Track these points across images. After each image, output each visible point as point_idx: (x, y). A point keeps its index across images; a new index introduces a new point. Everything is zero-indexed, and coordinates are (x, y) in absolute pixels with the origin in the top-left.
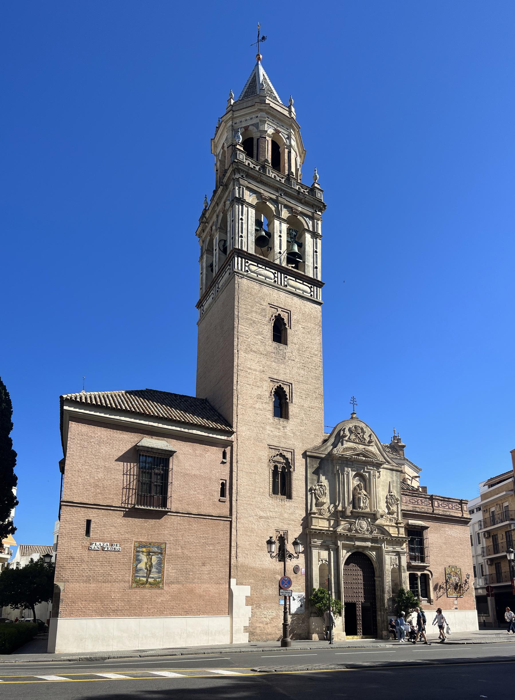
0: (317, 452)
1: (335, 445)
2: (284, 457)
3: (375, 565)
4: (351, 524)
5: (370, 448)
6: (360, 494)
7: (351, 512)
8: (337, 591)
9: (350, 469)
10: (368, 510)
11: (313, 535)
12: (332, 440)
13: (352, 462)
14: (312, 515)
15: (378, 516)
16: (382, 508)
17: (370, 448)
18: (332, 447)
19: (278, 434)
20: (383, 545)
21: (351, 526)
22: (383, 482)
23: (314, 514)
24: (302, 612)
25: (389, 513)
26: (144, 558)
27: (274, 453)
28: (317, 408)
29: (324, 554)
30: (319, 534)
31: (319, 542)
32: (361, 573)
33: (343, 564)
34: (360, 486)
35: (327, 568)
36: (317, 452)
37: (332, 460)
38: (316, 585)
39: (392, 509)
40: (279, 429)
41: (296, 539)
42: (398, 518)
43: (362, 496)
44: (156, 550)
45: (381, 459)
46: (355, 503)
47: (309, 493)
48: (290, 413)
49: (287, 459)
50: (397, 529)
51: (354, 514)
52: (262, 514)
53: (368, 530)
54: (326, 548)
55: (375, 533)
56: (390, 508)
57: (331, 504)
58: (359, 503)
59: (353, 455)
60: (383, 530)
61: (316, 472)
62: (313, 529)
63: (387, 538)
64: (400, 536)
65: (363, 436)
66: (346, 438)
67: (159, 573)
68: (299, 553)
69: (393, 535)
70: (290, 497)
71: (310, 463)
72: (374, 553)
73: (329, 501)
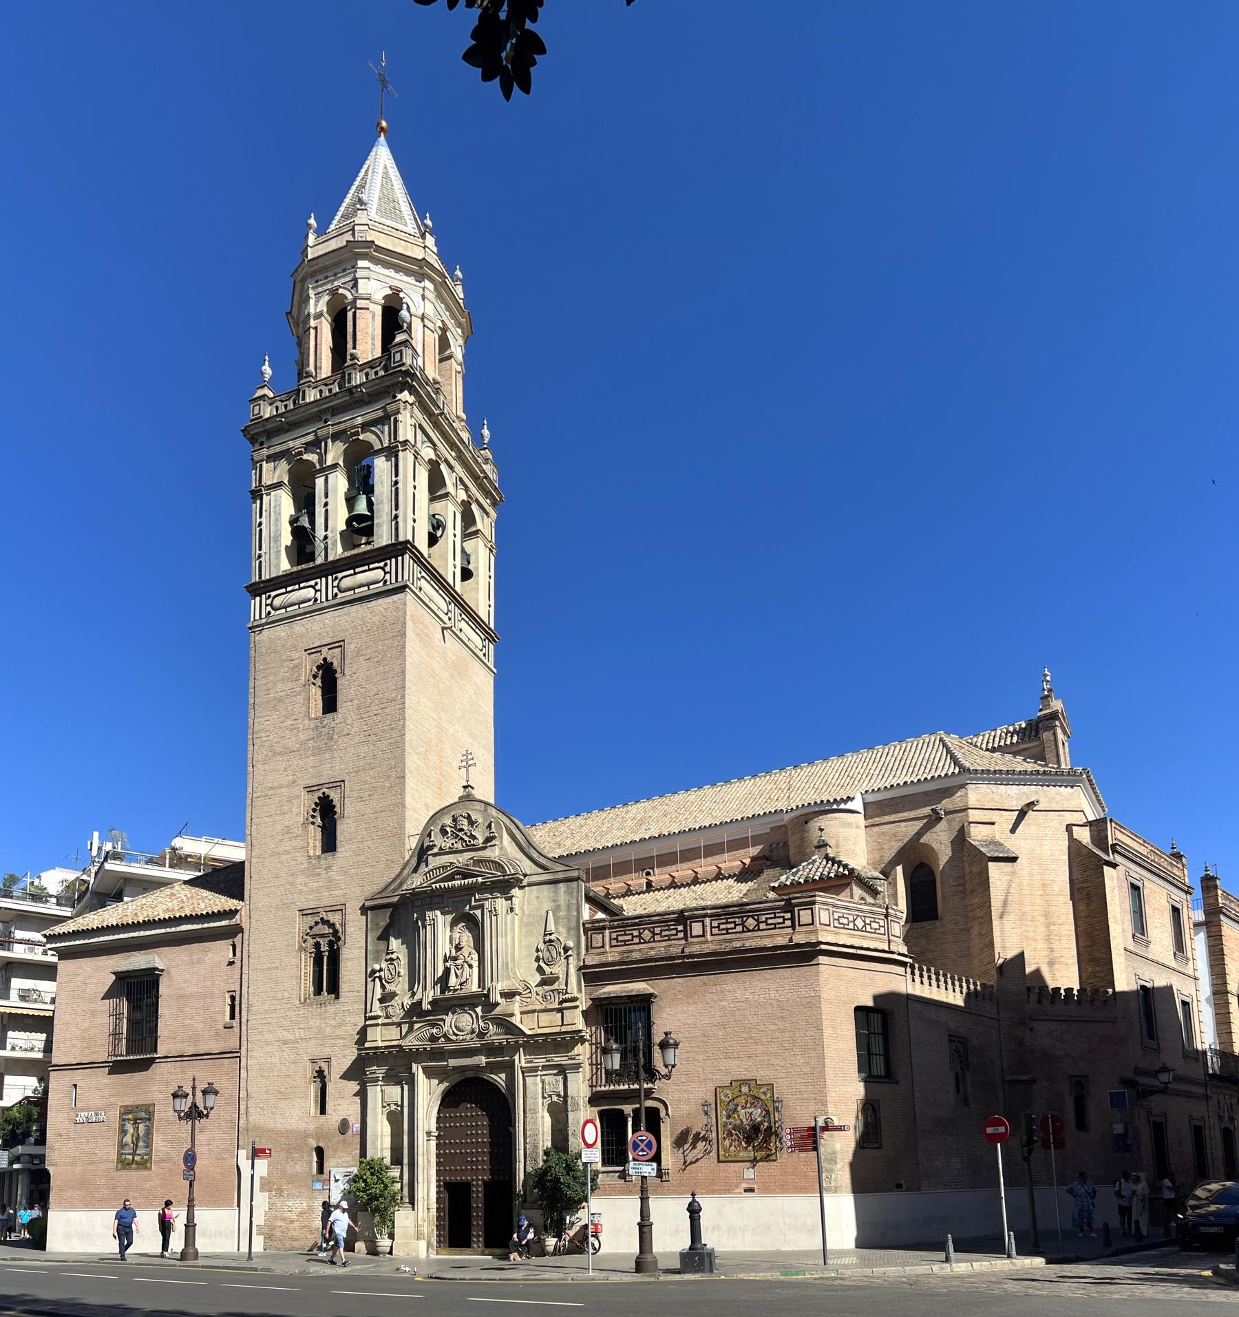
0: (384, 894)
26: (130, 1128)
27: (311, 920)
36: (384, 894)
40: (319, 875)
44: (143, 1115)
49: (332, 926)
52: (288, 1036)
67: (147, 1147)
72: (503, 1076)
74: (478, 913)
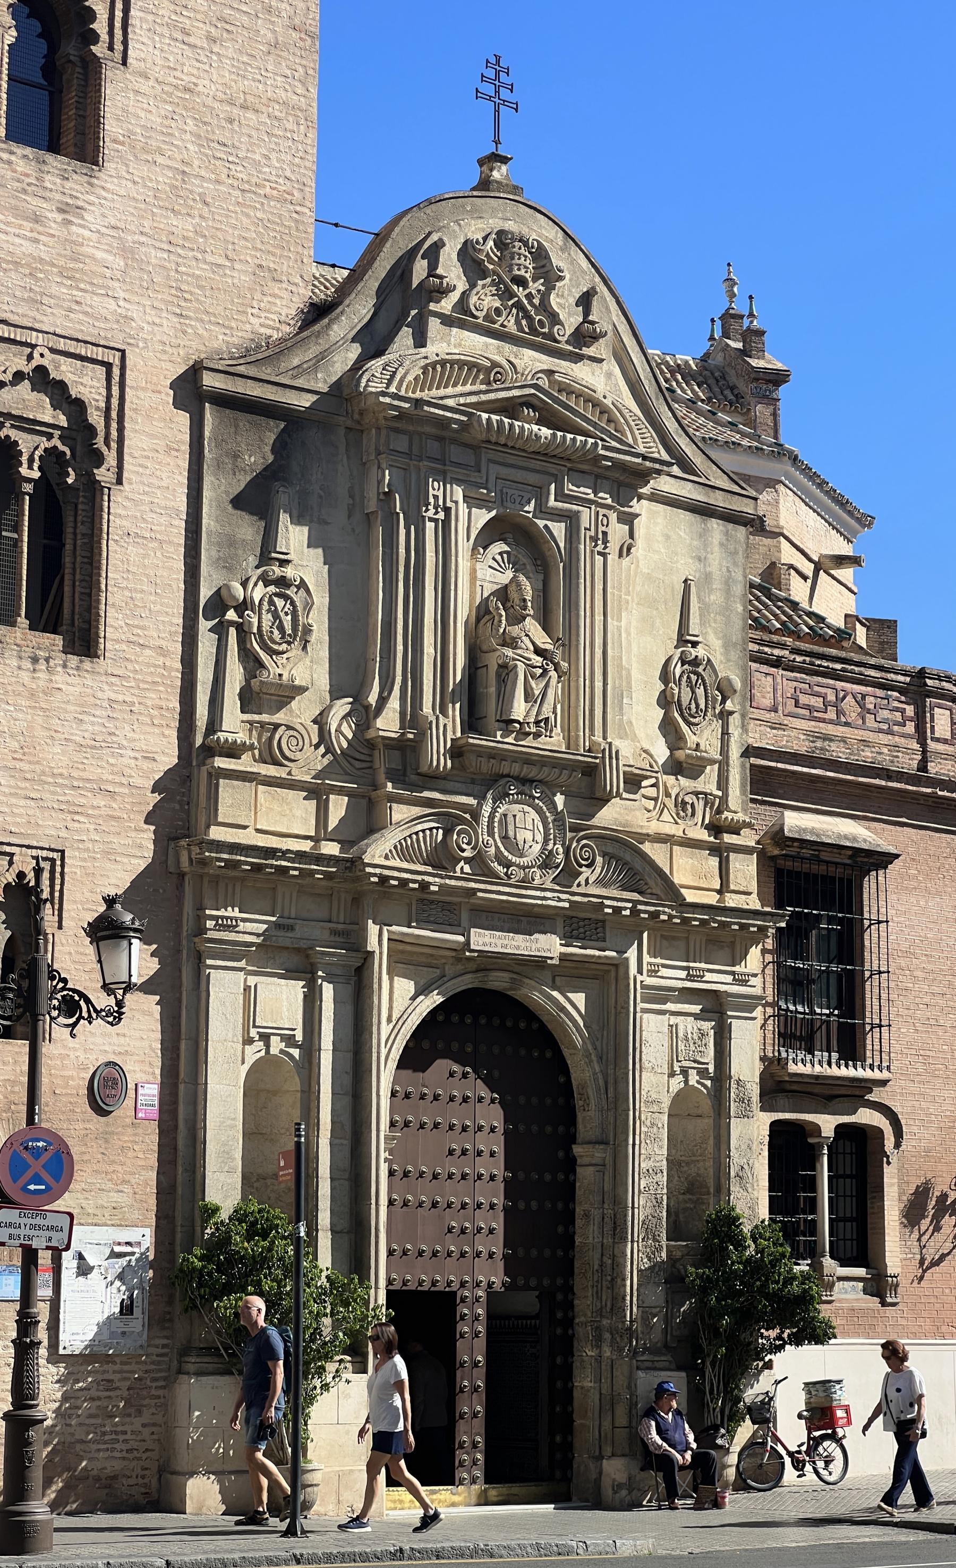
0: (266, 372)
1: (374, 341)
2: (58, 392)
3: (582, 1072)
4: (449, 822)
5: (583, 374)
6: (512, 643)
7: (457, 751)
8: (344, 1224)
9: (459, 492)
10: (554, 742)
11: (216, 880)
12: (359, 309)
13: (475, 448)
14: (221, 762)
15: (613, 779)
16: (637, 735)
17: (583, 374)
18: (355, 351)
19: (28, 248)
20: (632, 954)
21: (448, 832)
22: (649, 577)
23: (233, 751)
24: (127, 1346)
25: (676, 767)
28: (277, 110)
29: (282, 1000)
30: (259, 875)
31: (252, 927)
32: (494, 1116)
33: (392, 1064)
34: (513, 594)
35: (295, 1084)
36: (266, 372)
37: (356, 432)
38: (223, 1188)
39: (692, 740)
40: (37, 219)
41: (110, 902)
42: (724, 799)
43: (523, 658)
45: (645, 442)
46: (478, 695)
47: (204, 625)
48: (111, 127)
49: (75, 408)
50: (714, 862)
51: (471, 761)
53: (546, 863)
54: (295, 960)
55: (592, 883)
56: (680, 737)
57: (336, 693)
58: (505, 698)
59: (479, 406)
60: (638, 864)
61: (256, 500)
62: (219, 846)
63: (655, 915)
64: (732, 901)
65: (545, 297)
66: (446, 305)
68: (129, 987)
69: (691, 897)
70: (84, 642)
71: (219, 442)
72: (580, 999)
73: (323, 680)
74: (559, 529)
